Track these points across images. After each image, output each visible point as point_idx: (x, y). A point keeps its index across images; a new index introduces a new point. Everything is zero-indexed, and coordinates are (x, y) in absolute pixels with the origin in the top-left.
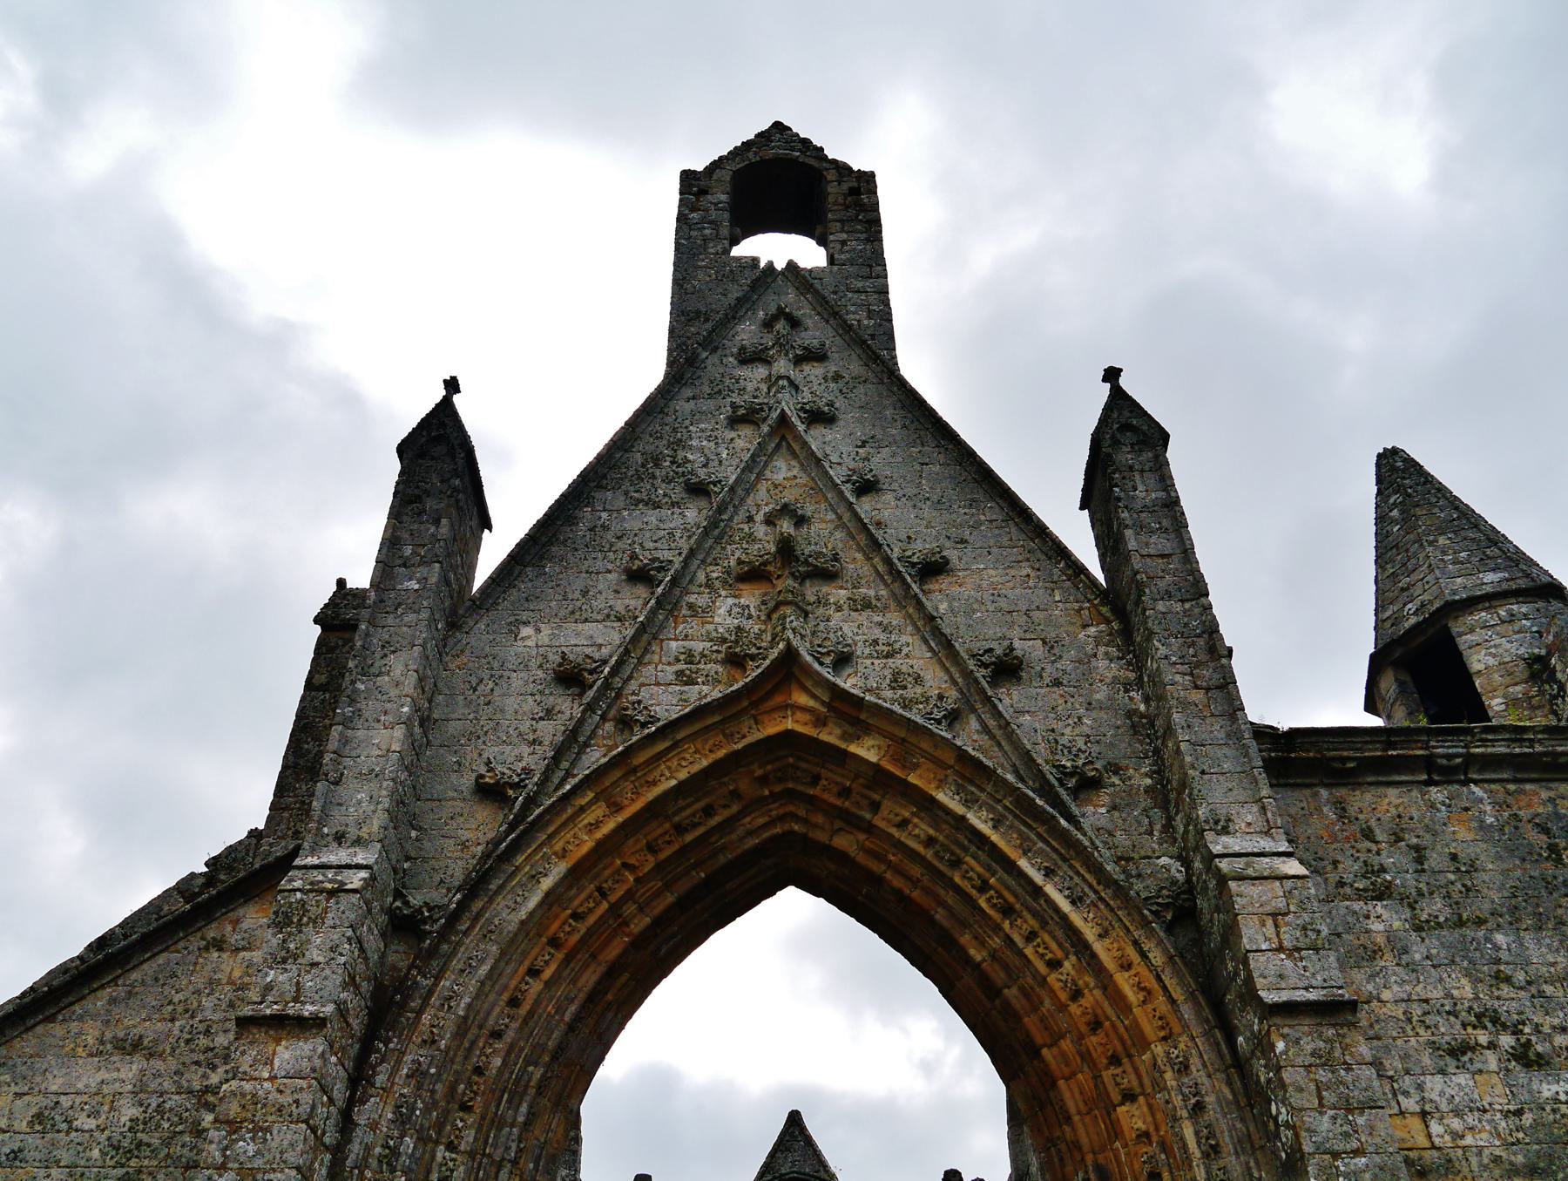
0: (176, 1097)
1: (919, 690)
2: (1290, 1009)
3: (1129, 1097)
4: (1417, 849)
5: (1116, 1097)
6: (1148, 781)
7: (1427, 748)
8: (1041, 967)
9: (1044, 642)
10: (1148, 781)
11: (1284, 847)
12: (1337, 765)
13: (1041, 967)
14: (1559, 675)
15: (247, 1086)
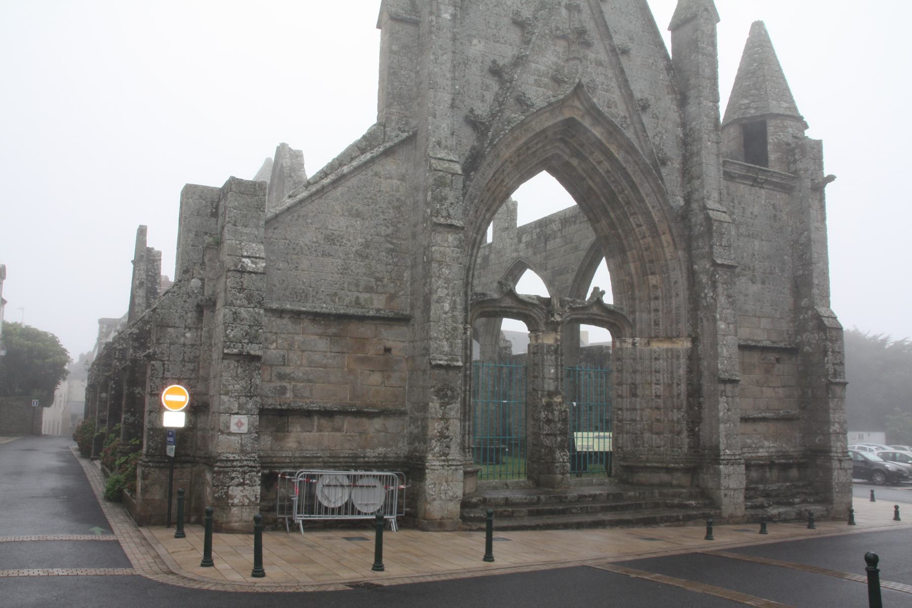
0: (376, 237)
1: (616, 111)
2: (722, 265)
3: (653, 273)
4: (744, 208)
5: (649, 272)
6: (678, 166)
7: (756, 175)
8: (634, 226)
9: (655, 98)
10: (678, 166)
11: (725, 210)
12: (733, 175)
13: (634, 226)
14: (796, 156)
15: (442, 249)
